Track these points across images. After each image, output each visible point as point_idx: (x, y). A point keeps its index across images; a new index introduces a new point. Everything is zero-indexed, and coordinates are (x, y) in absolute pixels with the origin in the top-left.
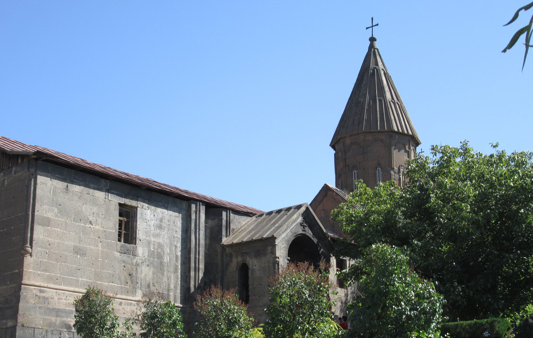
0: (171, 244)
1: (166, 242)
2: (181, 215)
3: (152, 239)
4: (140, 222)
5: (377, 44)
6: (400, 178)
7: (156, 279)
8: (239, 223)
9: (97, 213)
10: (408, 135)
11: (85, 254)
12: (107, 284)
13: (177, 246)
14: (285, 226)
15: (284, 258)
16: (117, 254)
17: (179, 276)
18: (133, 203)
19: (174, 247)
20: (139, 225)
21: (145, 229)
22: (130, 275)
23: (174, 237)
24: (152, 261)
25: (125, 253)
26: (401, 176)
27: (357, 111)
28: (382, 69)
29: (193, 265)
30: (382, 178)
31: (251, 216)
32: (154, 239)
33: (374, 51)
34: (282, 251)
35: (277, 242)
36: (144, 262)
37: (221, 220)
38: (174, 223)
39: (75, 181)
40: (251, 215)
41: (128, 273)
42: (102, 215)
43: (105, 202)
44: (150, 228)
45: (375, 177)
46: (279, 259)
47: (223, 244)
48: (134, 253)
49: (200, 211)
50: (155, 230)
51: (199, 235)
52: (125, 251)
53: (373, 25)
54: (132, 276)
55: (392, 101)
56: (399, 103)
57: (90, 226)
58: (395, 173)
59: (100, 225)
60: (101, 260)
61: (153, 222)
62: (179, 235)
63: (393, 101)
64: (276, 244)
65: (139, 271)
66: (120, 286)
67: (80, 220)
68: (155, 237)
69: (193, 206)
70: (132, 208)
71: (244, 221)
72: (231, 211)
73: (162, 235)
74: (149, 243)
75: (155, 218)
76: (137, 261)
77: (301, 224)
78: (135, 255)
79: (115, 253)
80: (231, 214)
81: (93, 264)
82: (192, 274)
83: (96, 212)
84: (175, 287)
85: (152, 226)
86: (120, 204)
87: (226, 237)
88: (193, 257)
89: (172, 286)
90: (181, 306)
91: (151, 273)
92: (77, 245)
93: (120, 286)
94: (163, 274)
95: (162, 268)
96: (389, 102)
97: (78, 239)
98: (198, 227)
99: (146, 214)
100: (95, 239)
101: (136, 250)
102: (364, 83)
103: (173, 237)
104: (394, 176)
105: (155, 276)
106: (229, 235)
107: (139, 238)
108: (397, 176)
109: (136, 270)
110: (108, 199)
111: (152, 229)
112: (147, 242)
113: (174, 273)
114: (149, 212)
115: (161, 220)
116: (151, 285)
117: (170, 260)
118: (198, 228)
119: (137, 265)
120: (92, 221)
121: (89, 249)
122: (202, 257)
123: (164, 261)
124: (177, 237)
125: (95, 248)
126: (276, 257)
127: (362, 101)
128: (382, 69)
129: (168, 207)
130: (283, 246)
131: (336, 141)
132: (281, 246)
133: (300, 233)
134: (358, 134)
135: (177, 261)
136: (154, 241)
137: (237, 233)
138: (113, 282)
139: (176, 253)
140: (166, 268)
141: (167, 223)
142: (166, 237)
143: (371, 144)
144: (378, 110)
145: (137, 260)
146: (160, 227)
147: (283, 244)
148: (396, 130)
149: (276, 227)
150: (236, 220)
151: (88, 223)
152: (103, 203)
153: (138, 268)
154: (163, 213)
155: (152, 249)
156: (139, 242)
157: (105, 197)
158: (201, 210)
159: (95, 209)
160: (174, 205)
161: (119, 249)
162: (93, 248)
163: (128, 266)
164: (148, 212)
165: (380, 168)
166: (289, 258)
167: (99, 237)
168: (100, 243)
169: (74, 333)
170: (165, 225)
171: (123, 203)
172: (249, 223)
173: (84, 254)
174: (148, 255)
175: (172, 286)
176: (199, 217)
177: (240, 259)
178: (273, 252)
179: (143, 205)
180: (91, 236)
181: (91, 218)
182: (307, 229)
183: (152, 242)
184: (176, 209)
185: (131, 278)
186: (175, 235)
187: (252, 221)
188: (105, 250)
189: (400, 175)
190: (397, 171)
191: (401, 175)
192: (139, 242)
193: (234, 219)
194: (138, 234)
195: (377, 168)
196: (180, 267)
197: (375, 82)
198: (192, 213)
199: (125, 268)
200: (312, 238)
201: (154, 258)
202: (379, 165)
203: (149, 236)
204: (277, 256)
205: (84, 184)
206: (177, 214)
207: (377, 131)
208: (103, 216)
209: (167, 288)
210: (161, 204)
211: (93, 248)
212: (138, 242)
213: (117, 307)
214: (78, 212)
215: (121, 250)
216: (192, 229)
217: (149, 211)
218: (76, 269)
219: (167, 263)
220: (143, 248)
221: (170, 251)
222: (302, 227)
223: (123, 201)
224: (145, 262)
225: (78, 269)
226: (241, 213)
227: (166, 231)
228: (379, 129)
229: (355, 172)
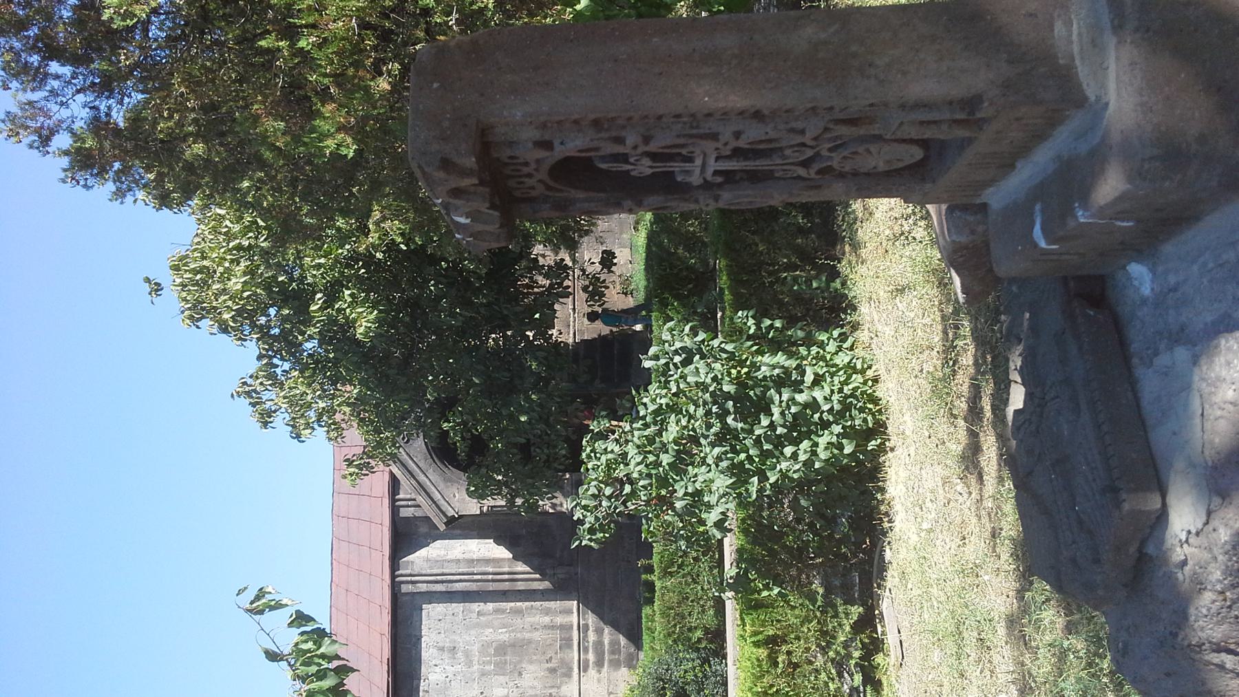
0: (478, 625)
2: (424, 606)
7: (538, 656)
17: (527, 603)
19: (481, 618)
29: (506, 586)
35: (451, 513)
36: (516, 682)
38: (440, 620)
62: (458, 607)
68: (471, 661)
69: (405, 588)
72: (397, 497)
75: (440, 662)
80: (401, 496)
82: (521, 586)
84: (547, 612)
85: (453, 669)
89: (547, 619)
90: (576, 602)
91: (532, 668)
94: (530, 642)
98: (438, 577)
103: (464, 622)
105: (535, 658)
112: (484, 679)
115: (442, 649)
116: (549, 665)
123: (505, 639)
124: (463, 612)
126: (481, 511)
129: (415, 636)
130: (457, 495)
135: (503, 611)
140: (519, 635)
146: (453, 650)
147: (454, 496)
155: (492, 667)
158: (408, 572)
160: (409, 622)
164: (433, 678)
170: (448, 640)
174: (504, 675)
175: (547, 619)
179: (424, 691)
184: (416, 618)
196: (512, 604)
203: (472, 673)
204: (478, 512)
206: (424, 613)
209: (550, 631)
210: (414, 652)
216: (444, 590)
219: (510, 632)
227: (457, 638)
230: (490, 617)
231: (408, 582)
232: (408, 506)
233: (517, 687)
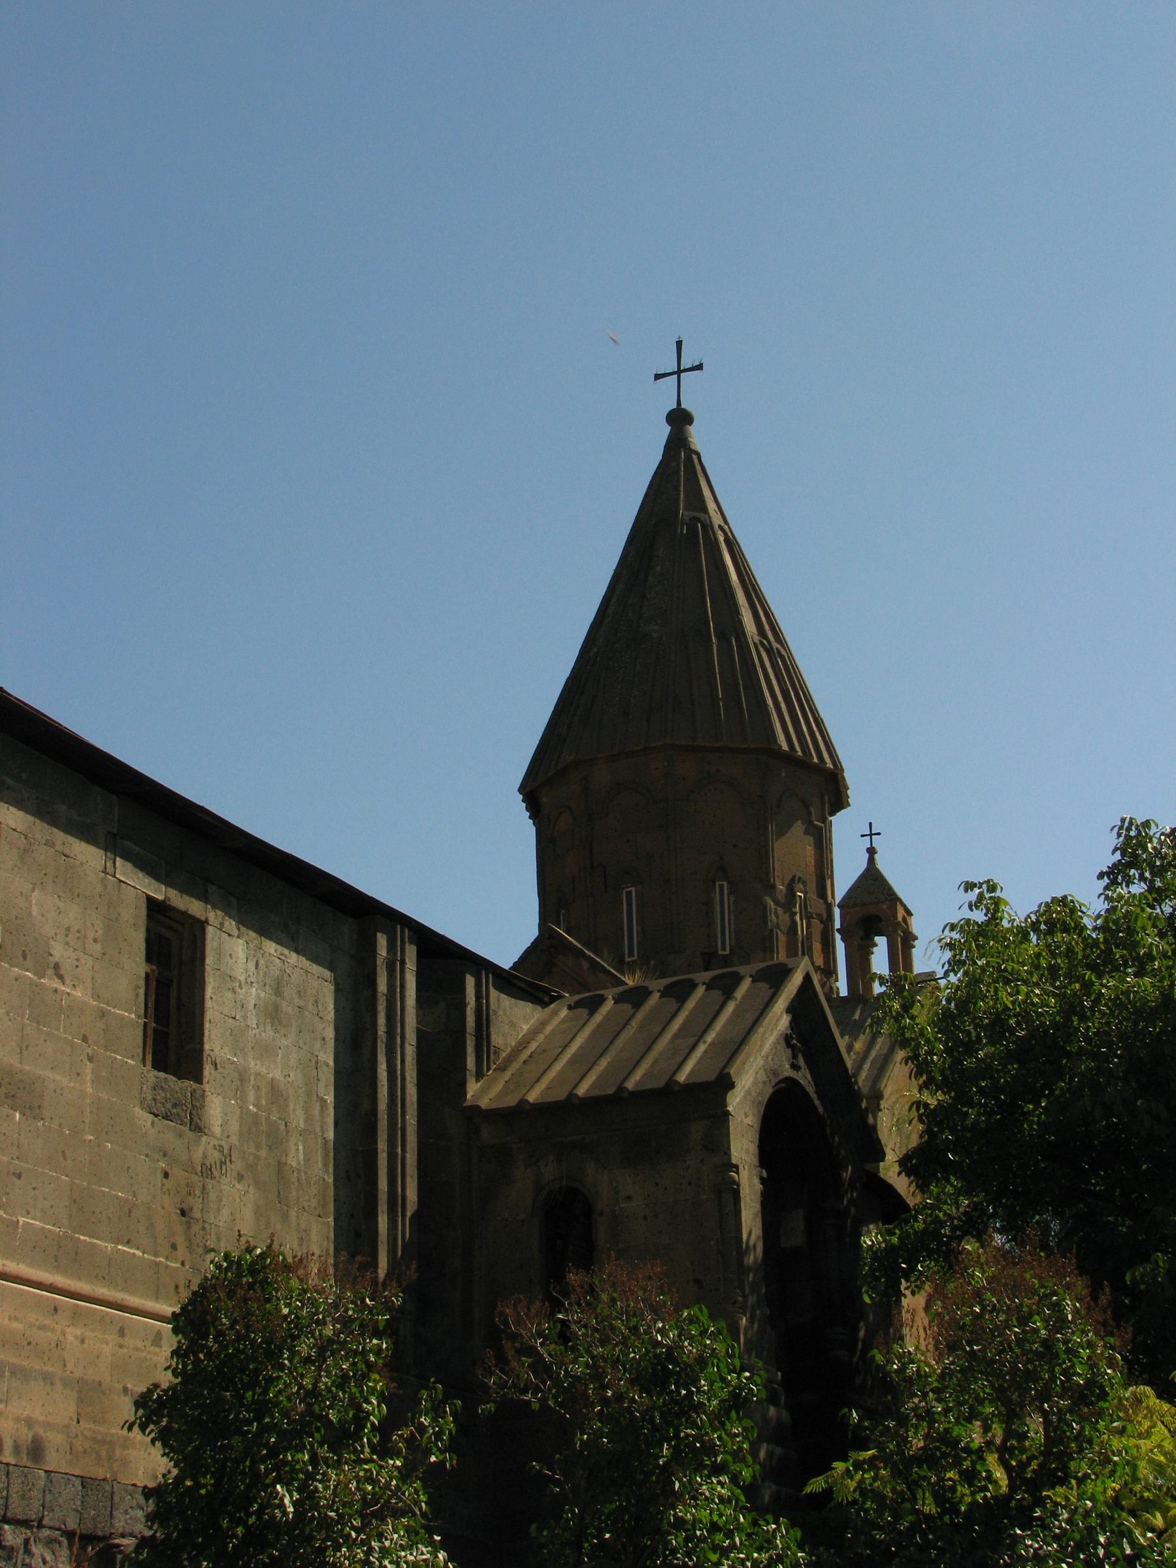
0: (309, 1094)
1: (293, 1081)
3: (253, 1065)
4: (213, 988)
5: (697, 435)
6: (794, 923)
8: (513, 1025)
9: (78, 931)
10: (820, 769)
11: (39, 1107)
12: (110, 1246)
13: (325, 1101)
14: (755, 1038)
15: (750, 1172)
16: (143, 1118)
18: (195, 907)
20: (211, 998)
21: (231, 1020)
22: (183, 1213)
23: (317, 1062)
24: (251, 1158)
25: (166, 1117)
26: (798, 918)
31: (544, 1004)
32: (258, 1062)
33: (689, 460)
34: (745, 1141)
36: (228, 1163)
37: (463, 1005)
38: (316, 1002)
39: (9, 781)
40: (547, 999)
41: (179, 1206)
42: (95, 941)
43: (105, 888)
44: (245, 1017)
46: (737, 1173)
47: (478, 1107)
48: (196, 1118)
49: (403, 963)
50: (262, 1028)
51: (403, 1061)
52: (169, 1106)
53: (682, 368)
54: (192, 1218)
56: (783, 653)
57: (56, 984)
58: (777, 903)
59: (89, 985)
60: (91, 1140)
61: (254, 990)
63: (765, 642)
64: (730, 1108)
65: (212, 1196)
66: (153, 1258)
67: (25, 957)
69: (382, 941)
70: (182, 924)
71: (526, 1019)
73: (280, 1052)
74: (242, 1076)
76: (205, 1157)
77: (787, 1039)
78: (198, 1128)
79: (138, 1110)
80: (492, 990)
81: (63, 1152)
83: (76, 929)
85: (251, 1007)
86: (150, 901)
87: (477, 1080)
88: (384, 1151)
92: (11, 1065)
93: (153, 1258)
94: (285, 1217)
95: (281, 1193)
96: (755, 644)
97: (15, 1038)
99: (231, 956)
100: (72, 1044)
101: (204, 1106)
102: (658, 568)
103: (314, 1059)
104: (777, 917)
106: (488, 1070)
107: (211, 1053)
108: (784, 919)
109: (203, 1193)
110: (114, 877)
111: (253, 1021)
113: (319, 1216)
114: (241, 948)
115: (278, 992)
117: (307, 1159)
118: (399, 1030)
119: (207, 1171)
120: (60, 965)
121: (52, 1087)
122: (411, 1157)
125: (72, 1084)
127: (655, 635)
128: (720, 526)
131: (549, 775)
132: (742, 1121)
133: (786, 1074)
135: (325, 1165)
136: (258, 1074)
137: (516, 1065)
138: (128, 1243)
139: (323, 1133)
141: (297, 1000)
142: (293, 1061)
145: (204, 1150)
148: (785, 746)
149: (712, 1044)
150: (505, 1014)
151: (50, 972)
152: (99, 889)
153: (210, 1183)
154: (283, 957)
156: (211, 1074)
157: (105, 868)
158: (407, 961)
159: (72, 913)
161: (149, 1097)
162: (64, 1081)
163: (176, 1172)
165: (725, 884)
166: (765, 1174)
167: (85, 1039)
168: (88, 1063)
169: (11, 1468)
170: (290, 1010)
171: (160, 897)
172: (549, 1029)
173: (33, 1111)
174: (241, 1134)
176: (403, 986)
177: (549, 1170)
178: (718, 1142)
179: (223, 919)
180: (58, 1030)
181: (58, 951)
182: (801, 1061)
183: (252, 1078)
185: (188, 1226)
186: (322, 1057)
187: (556, 1021)
188: (104, 1096)
189: (793, 914)
190: (781, 898)
192: (211, 1074)
193: (499, 1007)
194: (209, 1035)
195: (714, 882)
197: (701, 571)
198: (378, 968)
199: (169, 1184)
200: (817, 1102)
201: (258, 1147)
204: (734, 1161)
205: (37, 798)
208: (98, 947)
211: (64, 1081)
212: (208, 1070)
213: (149, 1352)
214: (16, 918)
215: (154, 1099)
217: (240, 941)
218: (8, 1173)
220: (224, 1098)
221: (306, 1121)
222: (789, 1051)
223: (159, 892)
224: (230, 1160)
225: (14, 1174)
226: (515, 985)
229: (629, 894)
230: (318, 1129)
231: (391, 947)
232: (478, 997)
233: (222, 1163)
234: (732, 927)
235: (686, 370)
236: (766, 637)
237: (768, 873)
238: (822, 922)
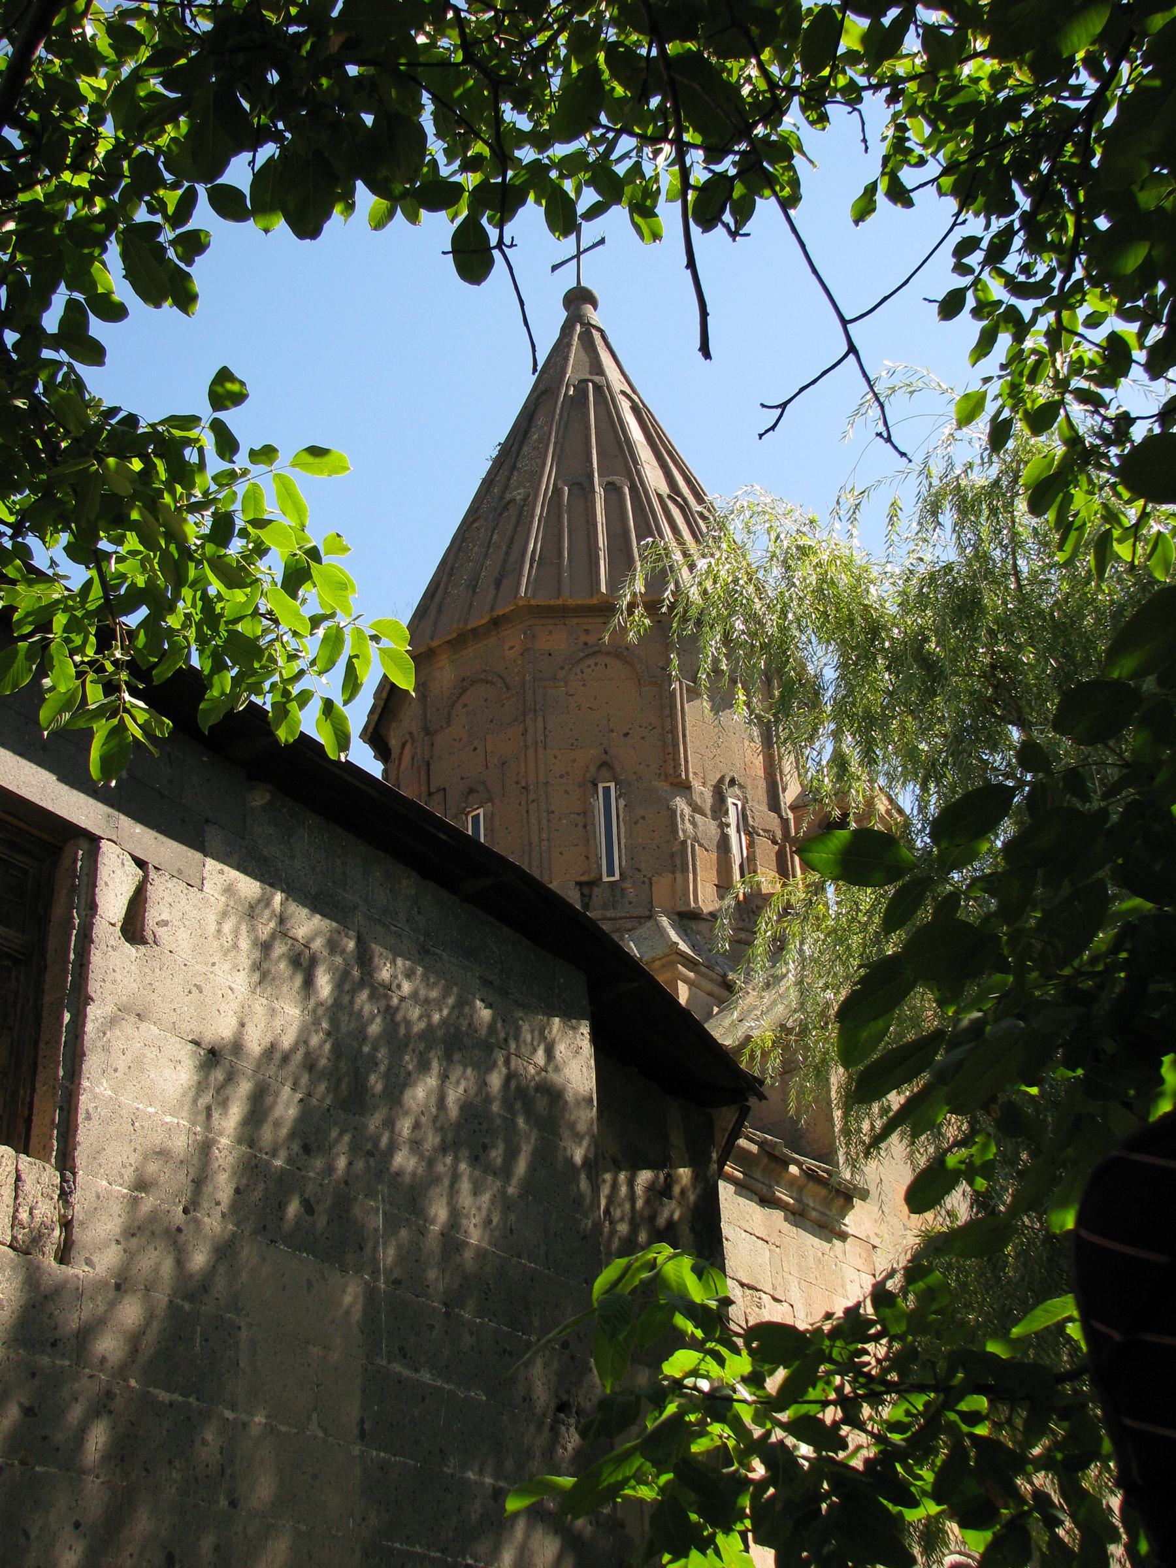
26: (732, 832)
27: (495, 537)
28: (623, 393)
30: (623, 829)
45: (585, 826)
55: (669, 497)
58: (696, 809)
104: (694, 824)
108: (707, 826)
127: (518, 497)
128: (623, 393)
134: (496, 623)
143: (562, 668)
144: (601, 545)
165: (612, 785)
189: (723, 826)
191: (728, 825)
195: (596, 785)
197: (588, 428)
202: (606, 765)
207: (595, 601)
228: (603, 589)
234: (623, 841)
235: (586, 250)
236: (680, 494)
237: (677, 765)
238: (774, 842)
